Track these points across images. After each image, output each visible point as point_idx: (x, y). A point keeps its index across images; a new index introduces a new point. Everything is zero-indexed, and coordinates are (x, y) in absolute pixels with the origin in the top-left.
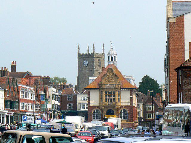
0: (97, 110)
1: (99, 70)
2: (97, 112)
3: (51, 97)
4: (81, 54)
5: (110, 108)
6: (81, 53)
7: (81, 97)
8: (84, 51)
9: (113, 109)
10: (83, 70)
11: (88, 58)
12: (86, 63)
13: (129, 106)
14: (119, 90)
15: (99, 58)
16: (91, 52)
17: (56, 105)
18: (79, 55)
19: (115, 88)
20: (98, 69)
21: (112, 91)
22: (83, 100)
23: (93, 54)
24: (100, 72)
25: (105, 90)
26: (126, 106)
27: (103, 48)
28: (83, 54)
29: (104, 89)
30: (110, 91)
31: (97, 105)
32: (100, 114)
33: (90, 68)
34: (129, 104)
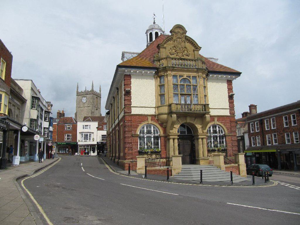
0: (149, 126)
2: (149, 132)
3: (29, 103)
5: (189, 120)
6: (80, 91)
8: (82, 89)
10: (82, 106)
11: (87, 95)
13: (227, 116)
14: (204, 76)
16: (89, 89)
17: (44, 128)
18: (78, 92)
21: (189, 77)
25: (173, 73)
26: (220, 117)
27: (100, 89)
30: (185, 77)
31: (152, 112)
33: (88, 104)
34: (227, 113)
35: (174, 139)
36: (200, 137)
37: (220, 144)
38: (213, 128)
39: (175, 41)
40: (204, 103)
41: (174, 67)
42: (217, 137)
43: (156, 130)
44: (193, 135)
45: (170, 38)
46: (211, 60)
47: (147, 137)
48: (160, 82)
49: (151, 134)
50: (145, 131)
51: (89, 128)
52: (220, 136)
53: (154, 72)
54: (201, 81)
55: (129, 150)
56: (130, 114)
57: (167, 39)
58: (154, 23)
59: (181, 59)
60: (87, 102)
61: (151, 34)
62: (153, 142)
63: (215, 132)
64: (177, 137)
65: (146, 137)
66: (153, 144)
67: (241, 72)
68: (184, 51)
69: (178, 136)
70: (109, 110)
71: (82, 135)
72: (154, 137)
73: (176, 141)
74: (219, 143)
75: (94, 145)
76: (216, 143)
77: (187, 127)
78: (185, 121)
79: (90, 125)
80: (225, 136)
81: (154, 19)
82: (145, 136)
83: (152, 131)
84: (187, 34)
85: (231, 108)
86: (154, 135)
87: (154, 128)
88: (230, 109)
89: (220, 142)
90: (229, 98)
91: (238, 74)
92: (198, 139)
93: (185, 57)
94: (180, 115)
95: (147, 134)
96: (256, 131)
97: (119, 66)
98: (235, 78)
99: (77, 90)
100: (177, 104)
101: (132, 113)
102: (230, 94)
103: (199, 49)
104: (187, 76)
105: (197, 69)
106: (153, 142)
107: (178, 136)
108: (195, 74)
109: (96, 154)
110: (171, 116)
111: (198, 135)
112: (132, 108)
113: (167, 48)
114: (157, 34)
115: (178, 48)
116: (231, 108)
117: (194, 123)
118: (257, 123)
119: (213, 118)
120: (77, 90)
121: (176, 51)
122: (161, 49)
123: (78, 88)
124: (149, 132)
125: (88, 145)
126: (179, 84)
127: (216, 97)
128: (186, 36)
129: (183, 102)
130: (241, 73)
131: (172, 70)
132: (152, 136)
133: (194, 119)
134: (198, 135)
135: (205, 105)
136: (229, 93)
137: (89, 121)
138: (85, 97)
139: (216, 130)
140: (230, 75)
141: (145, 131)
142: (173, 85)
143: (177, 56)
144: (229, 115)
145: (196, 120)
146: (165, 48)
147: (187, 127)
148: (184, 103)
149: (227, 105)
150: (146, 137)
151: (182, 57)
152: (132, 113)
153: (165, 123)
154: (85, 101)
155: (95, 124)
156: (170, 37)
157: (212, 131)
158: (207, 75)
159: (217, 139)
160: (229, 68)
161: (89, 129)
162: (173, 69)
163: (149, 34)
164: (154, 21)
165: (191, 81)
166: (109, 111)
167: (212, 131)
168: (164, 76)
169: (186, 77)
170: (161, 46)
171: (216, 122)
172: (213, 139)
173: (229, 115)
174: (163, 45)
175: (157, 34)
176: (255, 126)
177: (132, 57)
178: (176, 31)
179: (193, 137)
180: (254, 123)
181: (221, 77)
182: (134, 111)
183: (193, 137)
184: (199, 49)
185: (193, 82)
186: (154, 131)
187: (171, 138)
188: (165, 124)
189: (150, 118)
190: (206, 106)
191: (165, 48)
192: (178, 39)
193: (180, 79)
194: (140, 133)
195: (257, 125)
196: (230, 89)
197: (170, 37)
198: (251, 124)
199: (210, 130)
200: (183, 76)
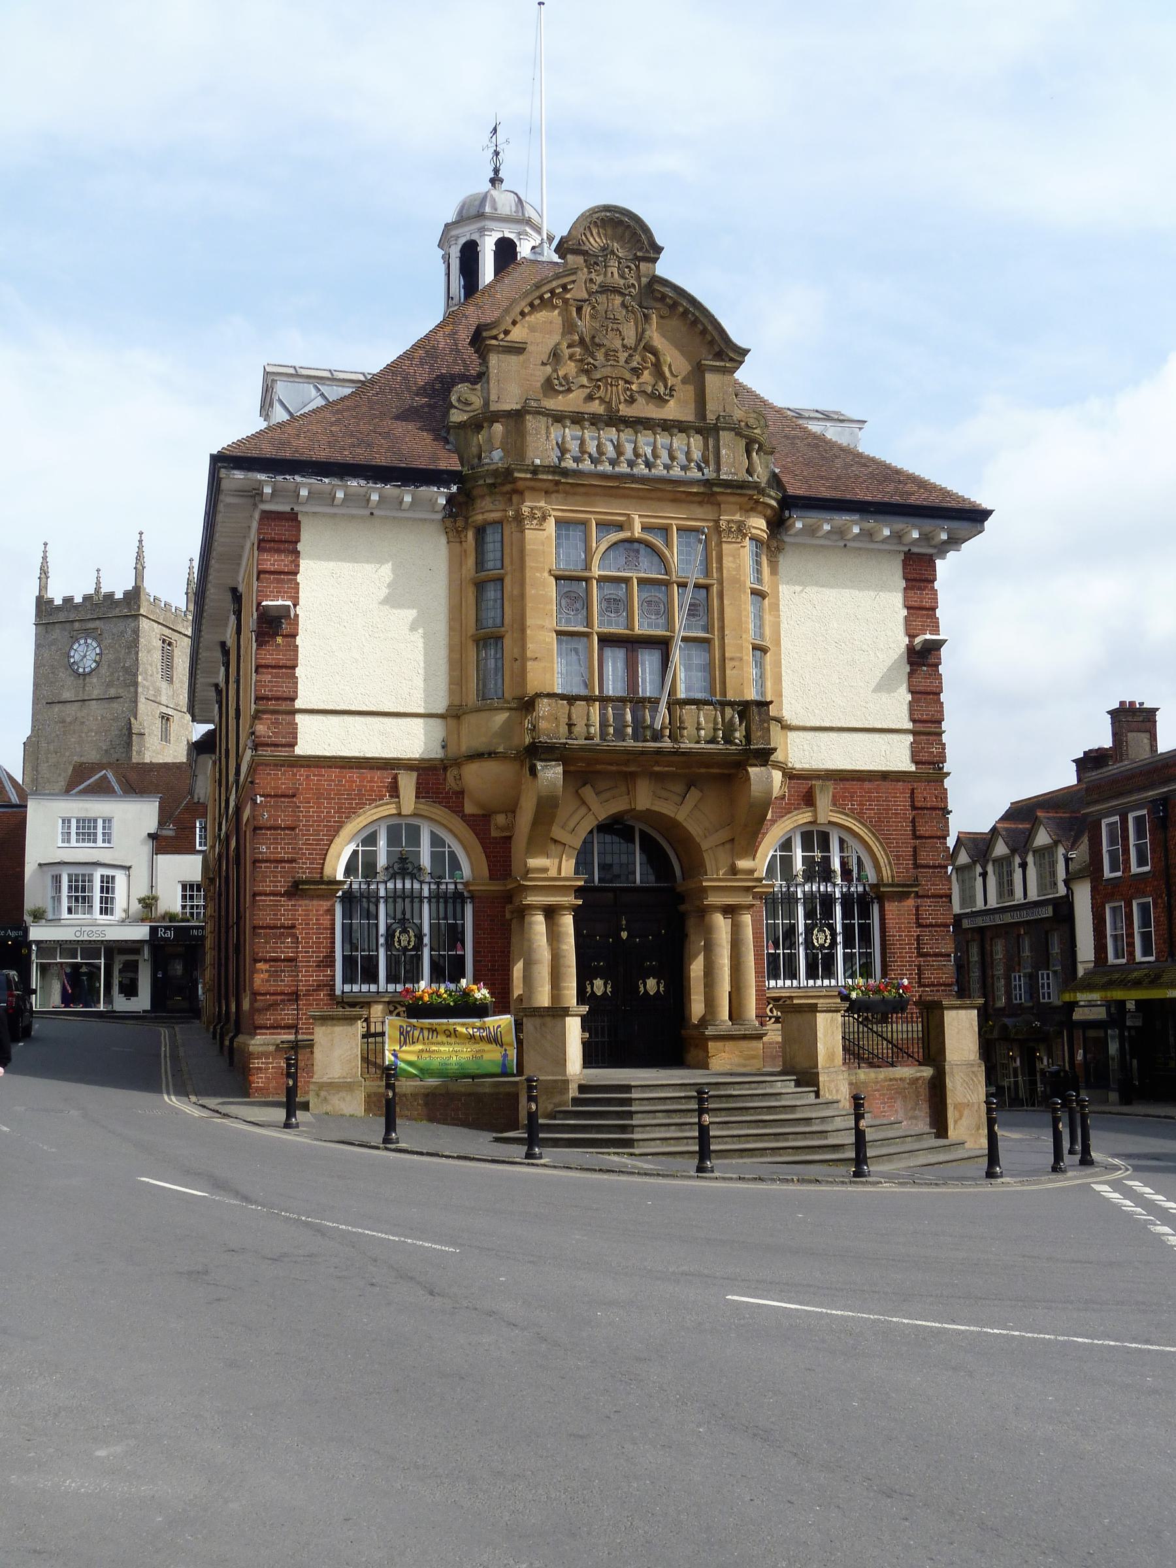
1: (164, 700)
2: (404, 866)
4: (58, 602)
5: (645, 798)
6: (57, 595)
7: (66, 821)
8: (70, 585)
9: (691, 814)
10: (67, 695)
11: (97, 623)
12: (85, 654)
14: (758, 524)
15: (167, 632)
16: (118, 585)
18: (43, 605)
19: (712, 492)
20: (158, 691)
21: (665, 530)
22: (74, 843)
23: (134, 596)
24: (170, 712)
28: (68, 600)
29: (561, 481)
32: (458, 898)
33: (109, 685)
34: (896, 755)
35: (551, 913)
36: (713, 899)
37: (848, 943)
38: (807, 846)
39: (587, 310)
40: (751, 694)
41: (565, 472)
42: (827, 901)
43: (452, 854)
44: (679, 889)
45: (552, 292)
46: (815, 427)
47: (394, 897)
48: (480, 564)
49: (413, 877)
50: (382, 861)
51: (100, 837)
52: (847, 900)
53: (442, 501)
54: (740, 559)
55: (275, 974)
56: (283, 752)
57: (537, 294)
58: (495, 180)
59: (614, 420)
60: (103, 670)
61: (470, 253)
62: (426, 929)
63: (819, 870)
64: (570, 900)
65: (386, 899)
66: (426, 940)
67: (986, 505)
68: (637, 372)
69: (579, 892)
70: (212, 727)
71: (57, 879)
72: (437, 897)
73: (567, 922)
74: (839, 939)
75: (131, 947)
76: (820, 938)
77: (645, 837)
78: (617, 806)
79: (107, 821)
80: (877, 895)
81: (497, 153)
82: (382, 893)
83: (426, 861)
84: (662, 269)
85: (920, 727)
86: (438, 884)
87: (436, 841)
88: (914, 733)
89: (848, 930)
90: (910, 663)
91: (973, 517)
92: (703, 912)
93: (644, 409)
94: (586, 767)
95: (393, 877)
96: (1135, 869)
97: (221, 462)
98: (955, 542)
99: (43, 587)
100: (571, 699)
101: (299, 750)
102: (918, 640)
103: (732, 360)
104: (645, 528)
105: (707, 483)
106: (426, 929)
107: (579, 892)
108: (698, 516)
109: (142, 1001)
110: (533, 772)
111: (704, 890)
112: (299, 718)
113: (530, 348)
114: (506, 250)
115: (600, 355)
116: (920, 727)
117: (681, 817)
118: (1139, 821)
119: (806, 786)
120: (43, 587)
121: (587, 372)
122: (493, 359)
123: (44, 572)
124: (404, 866)
125: (91, 948)
126: (596, 572)
127: (822, 657)
128: (657, 280)
129: (614, 686)
130: (984, 514)
131: (551, 486)
132: (426, 893)
133: (679, 788)
134: (704, 890)
135: (745, 709)
136: (912, 637)
137: (102, 790)
138: (88, 633)
139: (827, 860)
140: (919, 524)
141: (382, 861)
142: (557, 578)
143: (590, 398)
144: (913, 768)
145: (694, 795)
146: (518, 349)
147: (645, 837)
148: (621, 693)
149: (896, 707)
150: (386, 899)
151: (625, 410)
152: (299, 750)
153: (505, 812)
154: (89, 664)
155: (137, 817)
156: (554, 284)
157: (798, 866)
158: (777, 524)
159: (828, 913)
160: (922, 484)
161: (100, 843)
162: (557, 483)
163: (455, 252)
164: (496, 171)
165: (675, 557)
166: (214, 730)
167: (798, 866)
168: (500, 523)
169: (637, 532)
170: (495, 338)
171: (826, 812)
172: (807, 917)
173: (913, 768)
174: (507, 333)
175: (506, 250)
176: (1125, 838)
177: (320, 402)
178: (595, 242)
179: (681, 898)
180: (1124, 821)
181: (868, 535)
182: (315, 738)
183: (681, 898)
184: (732, 360)
185: (682, 559)
186: (436, 858)
187: (531, 907)
188: (500, 819)
189: (408, 784)
190: (755, 712)
191: (518, 349)
192: (602, 298)
193: (603, 547)
194: (350, 869)
195: (1140, 834)
196: (921, 609)
197: (554, 284)
198: (1104, 822)
199: (787, 862)
200: (620, 527)
